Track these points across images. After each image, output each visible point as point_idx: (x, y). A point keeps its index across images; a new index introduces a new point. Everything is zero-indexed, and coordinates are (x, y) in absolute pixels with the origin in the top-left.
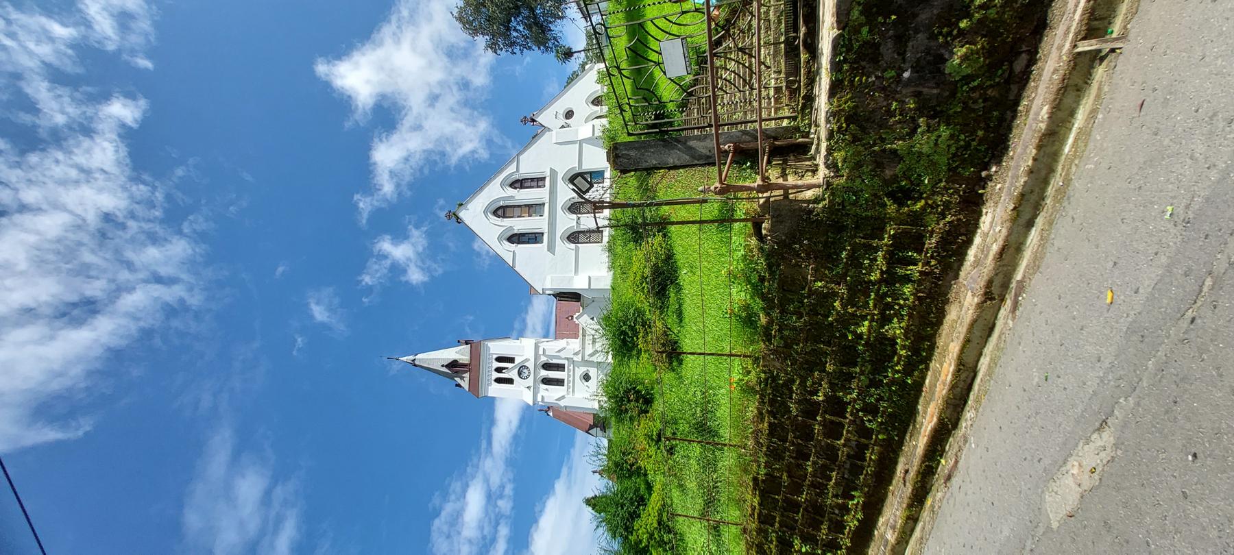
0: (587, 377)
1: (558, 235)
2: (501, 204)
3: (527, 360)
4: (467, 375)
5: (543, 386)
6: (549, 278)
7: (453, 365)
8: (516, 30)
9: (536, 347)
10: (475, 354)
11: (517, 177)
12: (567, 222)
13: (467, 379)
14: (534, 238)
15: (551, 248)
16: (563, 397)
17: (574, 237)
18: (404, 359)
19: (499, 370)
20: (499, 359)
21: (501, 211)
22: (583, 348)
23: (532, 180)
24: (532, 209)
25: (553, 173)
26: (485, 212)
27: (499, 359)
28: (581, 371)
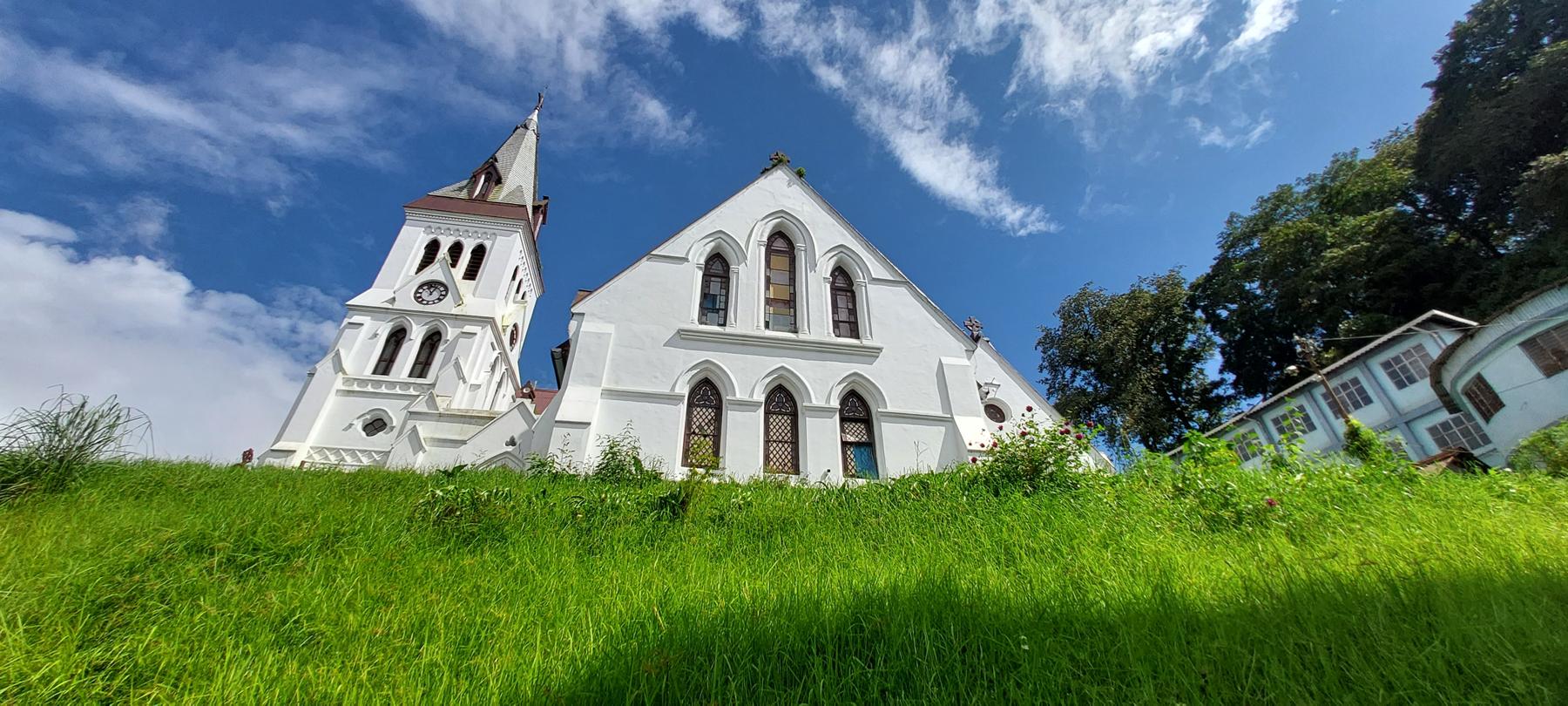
0: (375, 425)
1: (717, 358)
2: (799, 245)
3: (459, 301)
4: (464, 194)
5: (384, 330)
6: (610, 328)
7: (495, 178)
8: (1074, 375)
9: (488, 321)
10: (511, 211)
11: (859, 278)
12: (747, 379)
13: (453, 195)
14: (714, 303)
15: (684, 337)
16: (338, 367)
17: (707, 394)
18: (535, 117)
19: (456, 250)
20: (479, 253)
21: (783, 244)
22: (441, 417)
23: (853, 312)
24: (785, 305)
25: (873, 353)
26: (782, 213)
27: (479, 253)
28: (395, 412)
